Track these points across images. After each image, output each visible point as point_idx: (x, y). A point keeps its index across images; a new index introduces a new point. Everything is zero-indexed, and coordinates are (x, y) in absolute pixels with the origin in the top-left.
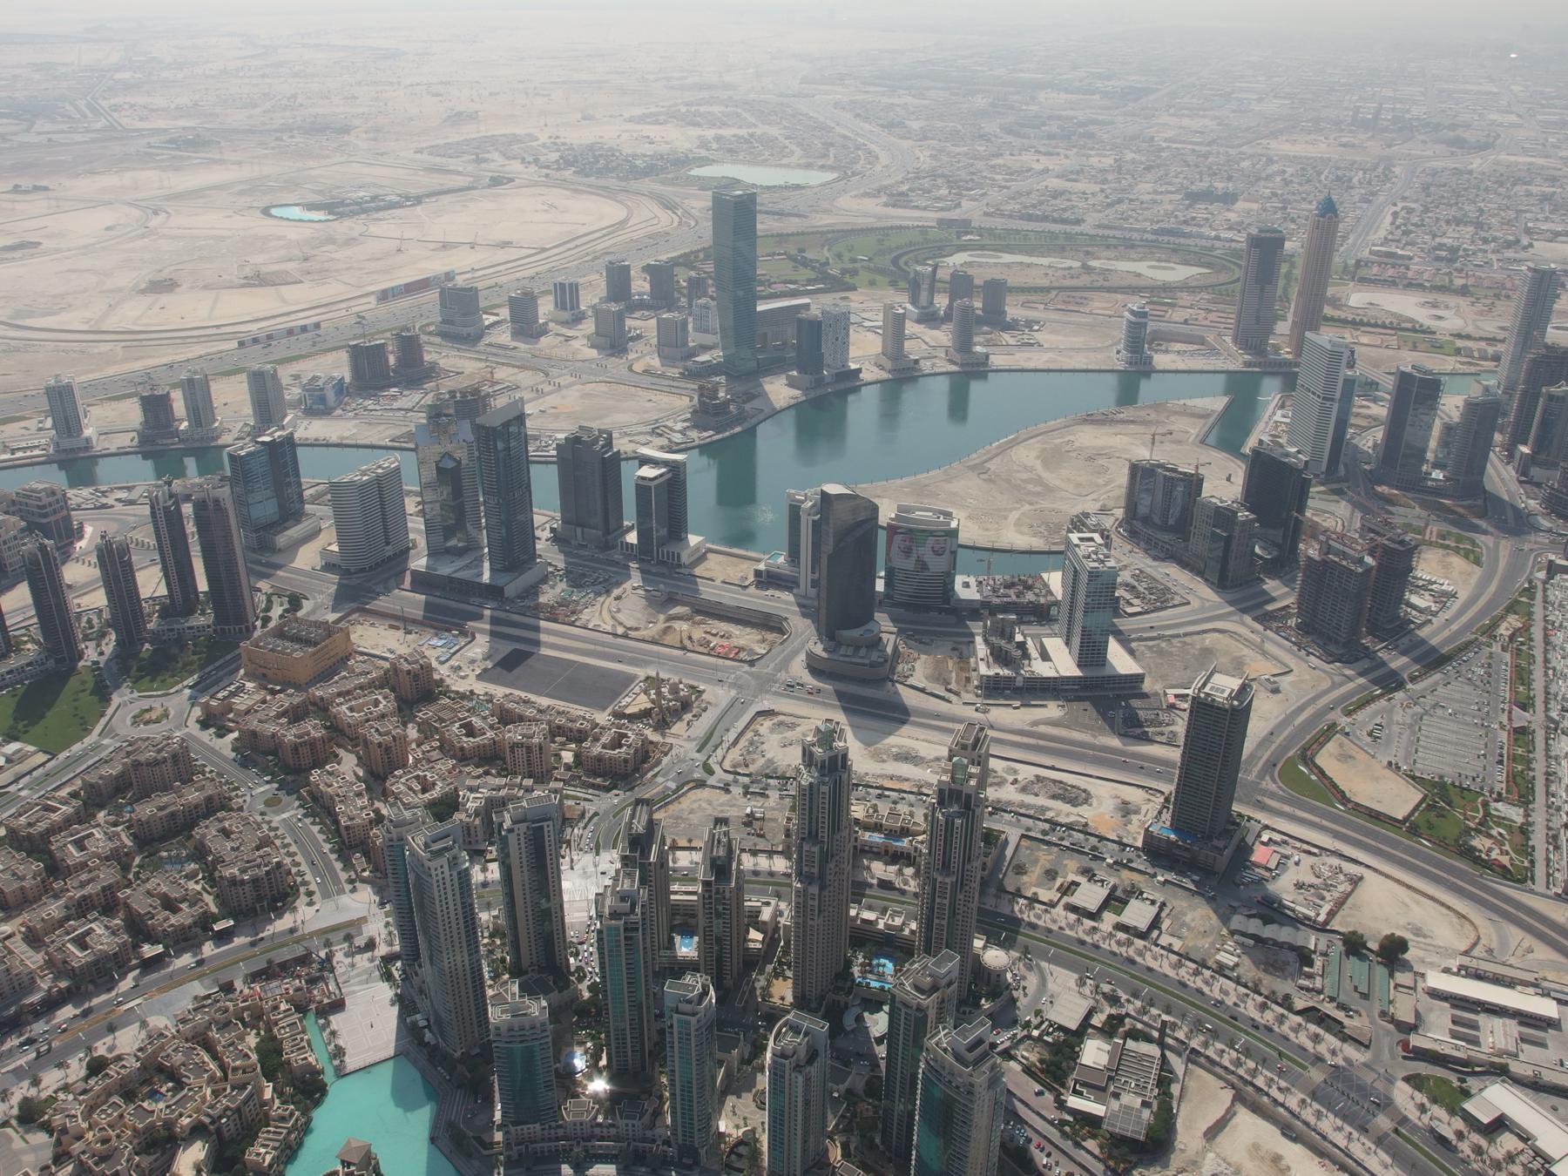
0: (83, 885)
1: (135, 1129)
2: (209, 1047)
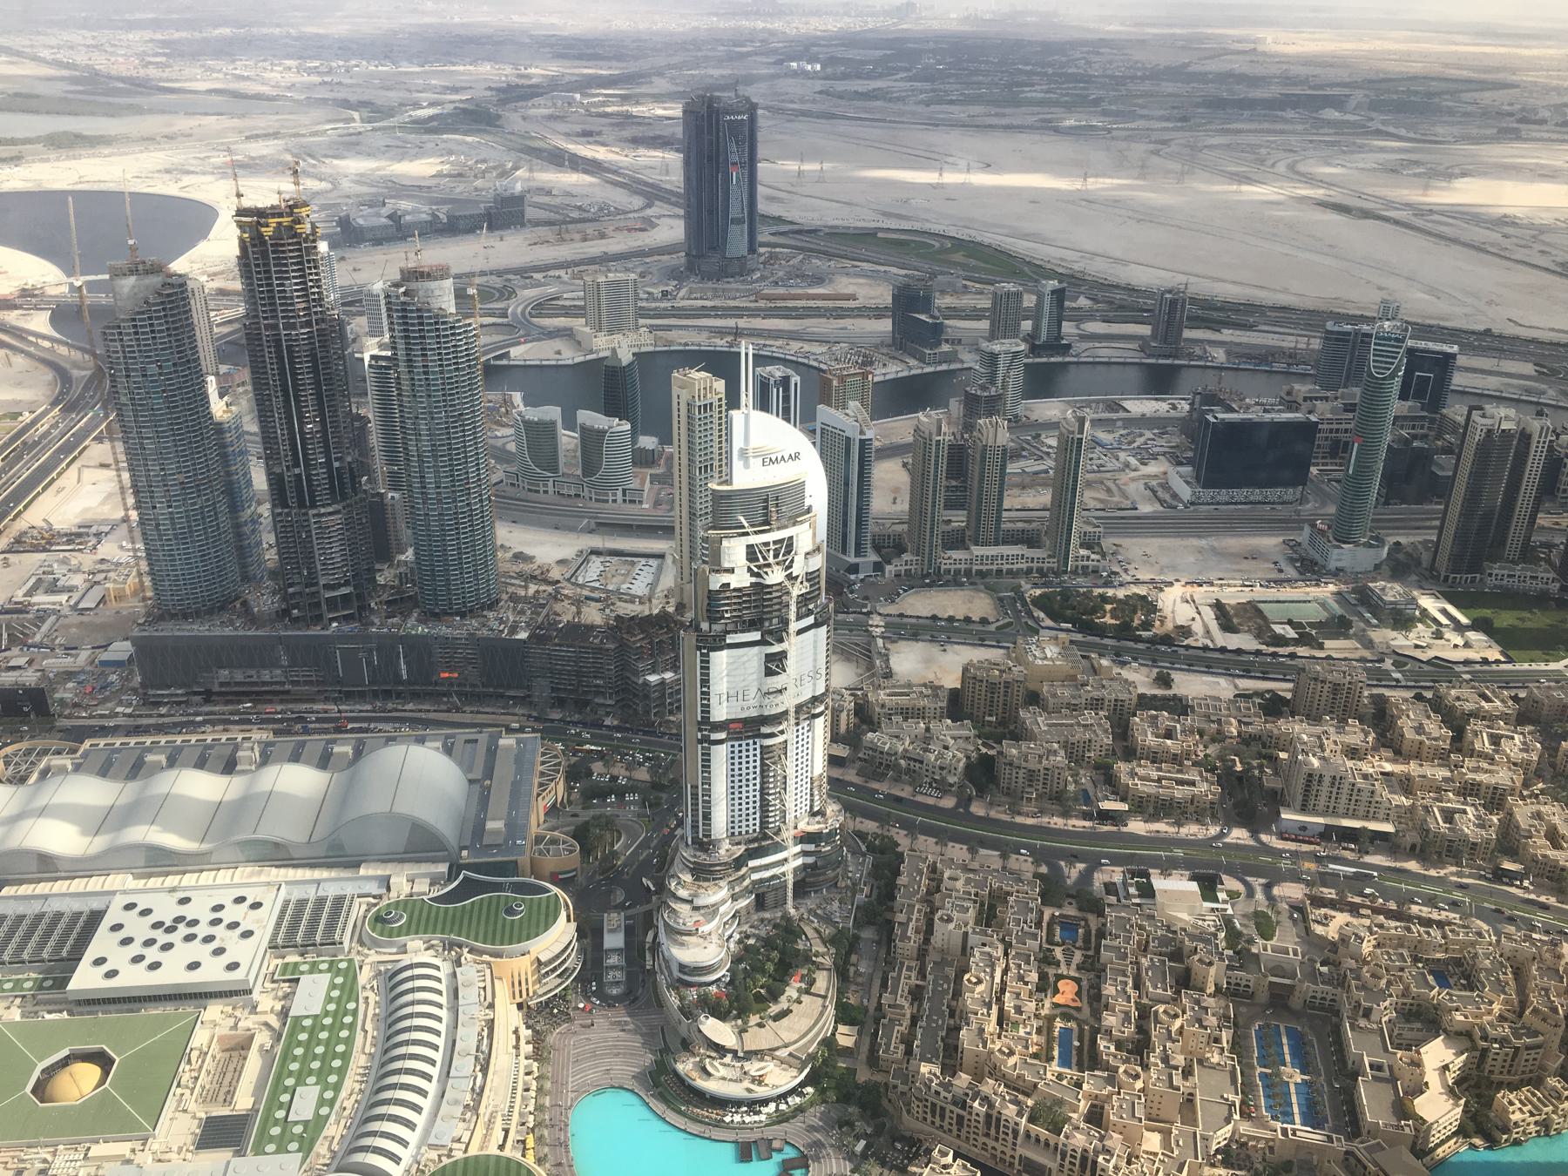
0: (1477, 770)
1: (1407, 988)
2: (1519, 973)
